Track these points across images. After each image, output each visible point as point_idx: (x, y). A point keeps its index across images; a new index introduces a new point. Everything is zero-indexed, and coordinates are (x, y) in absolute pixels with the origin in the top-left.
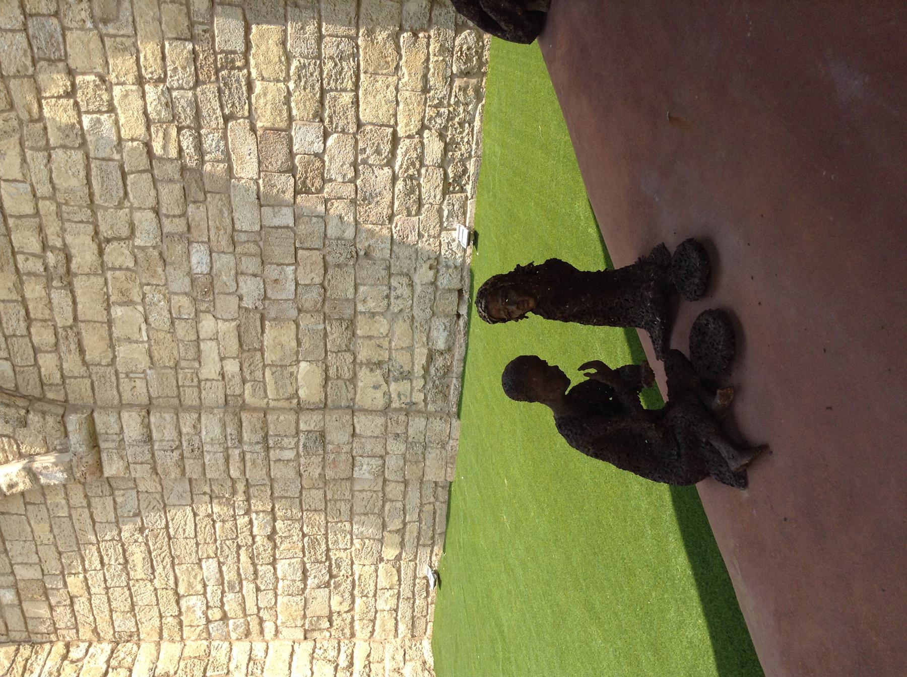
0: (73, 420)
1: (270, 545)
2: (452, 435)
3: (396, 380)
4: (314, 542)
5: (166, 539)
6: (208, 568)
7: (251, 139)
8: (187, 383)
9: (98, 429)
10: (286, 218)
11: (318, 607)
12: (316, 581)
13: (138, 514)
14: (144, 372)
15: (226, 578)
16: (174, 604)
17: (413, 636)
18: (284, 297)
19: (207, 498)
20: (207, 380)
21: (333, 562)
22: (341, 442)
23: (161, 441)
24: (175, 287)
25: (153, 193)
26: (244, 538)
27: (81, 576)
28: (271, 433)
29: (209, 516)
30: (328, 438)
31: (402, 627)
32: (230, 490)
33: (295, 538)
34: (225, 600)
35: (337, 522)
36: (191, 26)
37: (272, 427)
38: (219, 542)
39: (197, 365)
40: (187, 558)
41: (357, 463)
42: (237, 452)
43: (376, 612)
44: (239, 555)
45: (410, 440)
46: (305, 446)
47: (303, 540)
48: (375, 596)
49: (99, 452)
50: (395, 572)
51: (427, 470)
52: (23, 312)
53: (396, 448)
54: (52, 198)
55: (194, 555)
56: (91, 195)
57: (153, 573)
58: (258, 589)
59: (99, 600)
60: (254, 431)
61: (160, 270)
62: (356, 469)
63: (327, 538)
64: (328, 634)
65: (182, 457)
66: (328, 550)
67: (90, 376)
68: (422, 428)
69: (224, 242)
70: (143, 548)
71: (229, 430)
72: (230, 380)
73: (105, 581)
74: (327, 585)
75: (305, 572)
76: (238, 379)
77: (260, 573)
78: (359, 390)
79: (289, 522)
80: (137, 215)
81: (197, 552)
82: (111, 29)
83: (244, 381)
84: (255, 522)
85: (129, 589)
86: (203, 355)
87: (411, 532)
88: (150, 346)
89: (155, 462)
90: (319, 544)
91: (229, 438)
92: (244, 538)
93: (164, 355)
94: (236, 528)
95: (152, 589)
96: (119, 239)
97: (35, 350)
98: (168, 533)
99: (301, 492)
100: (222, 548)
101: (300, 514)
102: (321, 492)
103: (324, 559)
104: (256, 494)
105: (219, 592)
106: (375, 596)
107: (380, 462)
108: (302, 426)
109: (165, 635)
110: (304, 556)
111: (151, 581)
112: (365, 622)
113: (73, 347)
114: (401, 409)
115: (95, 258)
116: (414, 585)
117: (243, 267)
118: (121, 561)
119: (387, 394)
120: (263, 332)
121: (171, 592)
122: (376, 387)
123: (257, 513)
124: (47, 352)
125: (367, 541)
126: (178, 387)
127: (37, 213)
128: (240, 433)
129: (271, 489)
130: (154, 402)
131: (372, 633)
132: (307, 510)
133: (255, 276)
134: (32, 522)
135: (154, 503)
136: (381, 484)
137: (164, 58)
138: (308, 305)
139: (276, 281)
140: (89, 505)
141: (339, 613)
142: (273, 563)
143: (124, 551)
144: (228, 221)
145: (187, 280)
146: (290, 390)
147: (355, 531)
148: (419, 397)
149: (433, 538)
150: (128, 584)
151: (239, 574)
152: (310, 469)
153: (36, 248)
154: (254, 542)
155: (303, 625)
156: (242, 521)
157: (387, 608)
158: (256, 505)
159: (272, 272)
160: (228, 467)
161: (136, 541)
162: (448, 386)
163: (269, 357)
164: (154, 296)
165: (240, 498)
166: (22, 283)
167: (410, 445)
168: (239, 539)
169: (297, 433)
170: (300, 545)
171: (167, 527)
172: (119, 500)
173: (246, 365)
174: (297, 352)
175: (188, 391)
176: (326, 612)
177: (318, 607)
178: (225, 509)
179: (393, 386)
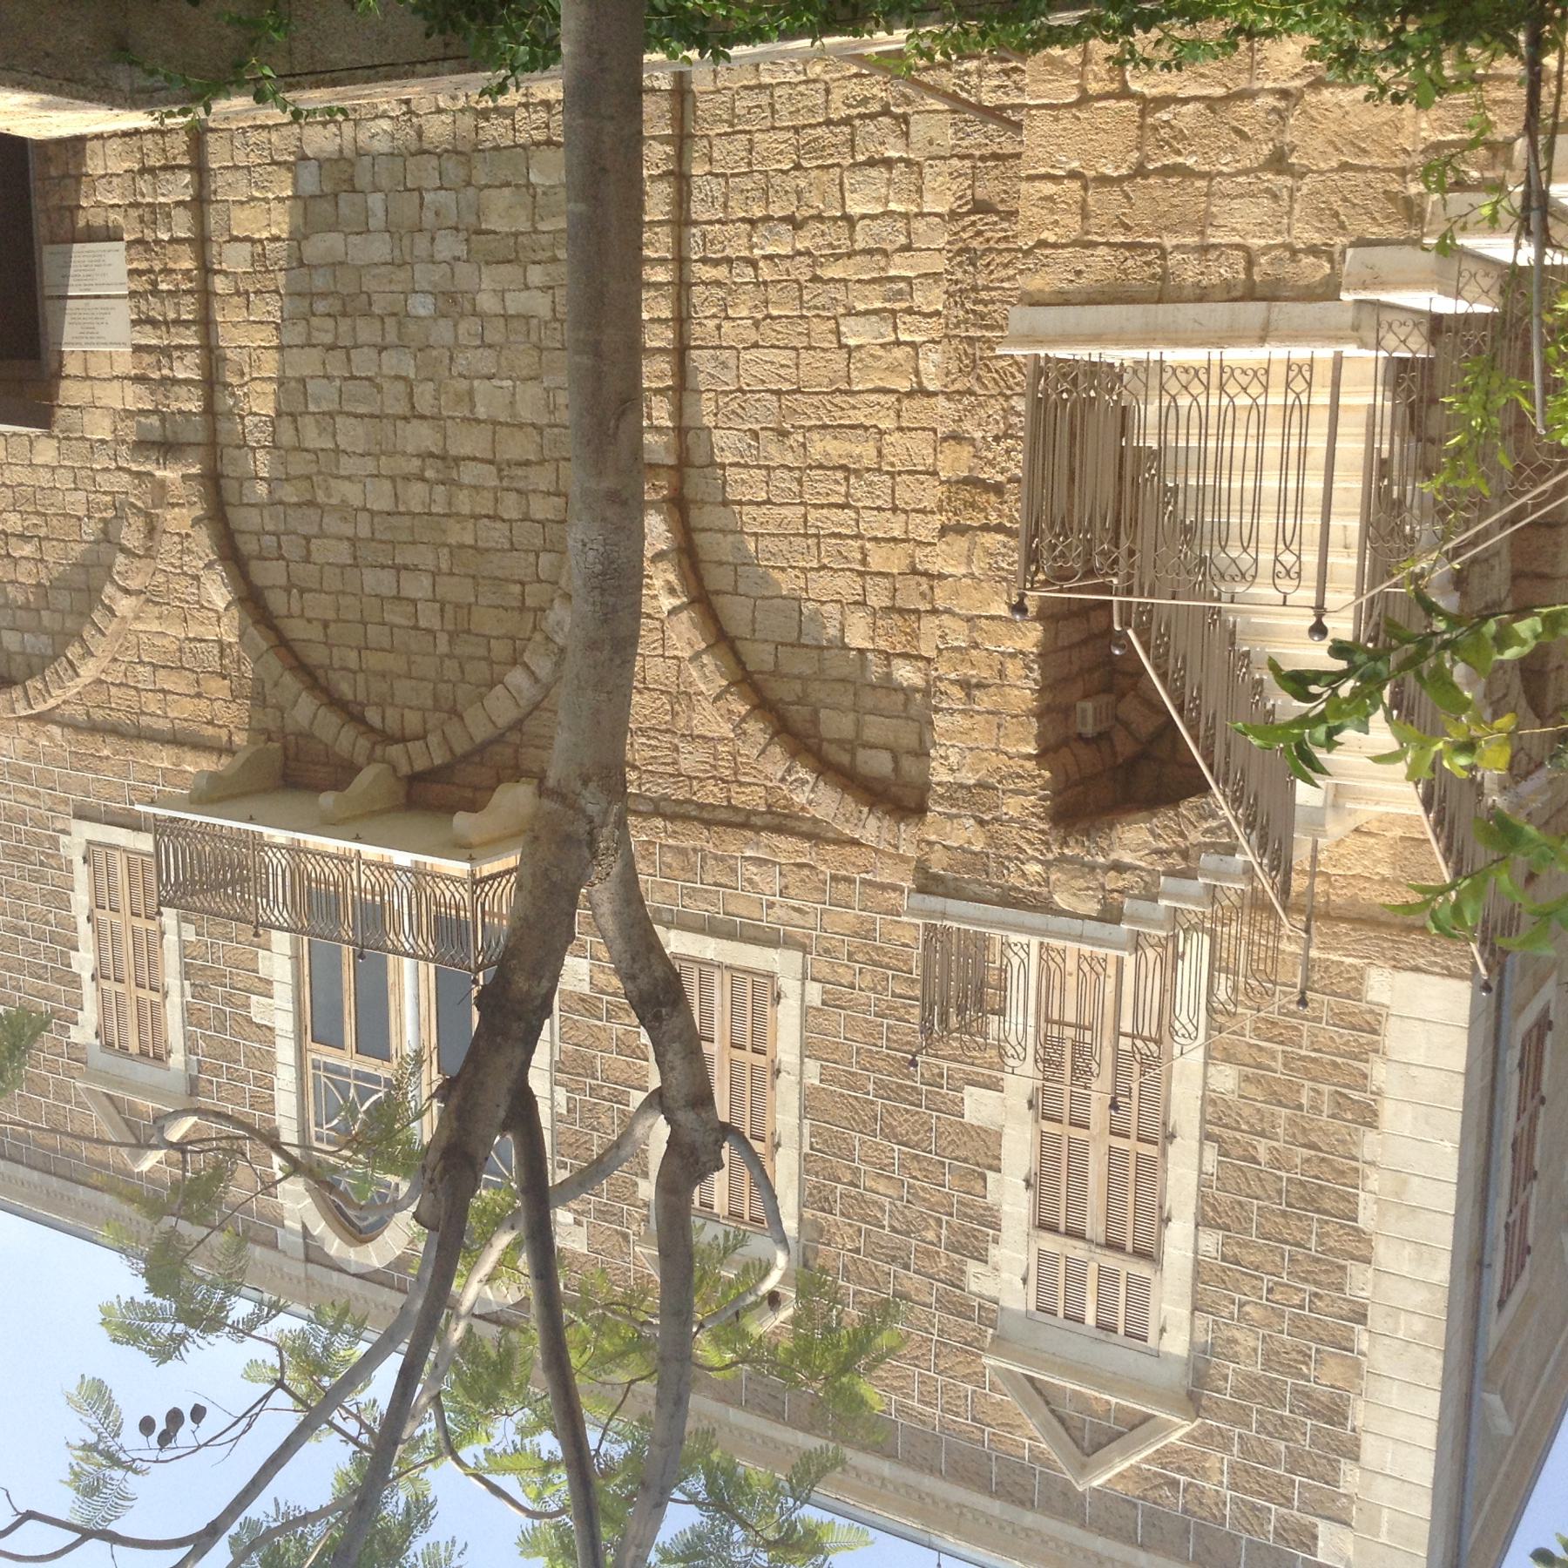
1: (815, 226)
5: (798, 396)
6: (856, 334)
7: (315, 238)
10: (376, 201)
12: (891, 140)
14: (547, 390)
15: (878, 305)
16: (933, 400)
18: (454, 205)
20: (554, 310)
21: (854, 112)
24: (448, 337)
25: (366, 349)
27: (868, 545)
29: (756, 324)
34: (926, 309)
35: (774, 111)
36: (238, 293)
38: (805, 312)
39: (535, 321)
40: (836, 367)
44: (832, 280)
47: (806, 169)
52: (486, 520)
54: (377, 457)
55: (828, 355)
56: (372, 416)
57: (866, 428)
58: (907, 248)
61: (435, 353)
63: (804, 127)
66: (829, 122)
67: (557, 460)
69: (402, 275)
70: (815, 436)
72: (553, 279)
73: (879, 509)
74: (905, 118)
75: (871, 163)
76: (551, 268)
79: (771, 192)
80: (385, 370)
81: (824, 350)
82: (246, 370)
84: (770, 250)
85: (900, 473)
86: (522, 311)
88: (518, 378)
90: (815, 140)
93: (526, 362)
94: (779, 282)
95: (897, 435)
96: (411, 395)
97: (526, 518)
98: (788, 392)
99: (717, 175)
100: (816, 308)
101: (757, 176)
103: (847, 130)
105: (908, 318)
110: (838, 165)
111: (881, 433)
113: (520, 472)
115: (425, 424)
117: (424, 254)
118: (840, 475)
120: (495, 232)
121: (906, 403)
123: (751, 248)
124: (528, 505)
127: (392, 478)
132: (750, 164)
133: (433, 239)
137: (262, 323)
138: (462, 173)
139: (437, 214)
143: (821, 467)
144: (383, 269)
145: (442, 322)
150: (888, 473)
151: (873, 281)
153: (418, 488)
154: (808, 253)
156: (766, 273)
159: (429, 218)
161: (804, 445)
163: (524, 226)
164: (461, 364)
166: (458, 514)
168: (802, 279)
170: (814, 173)
171: (778, 393)
174: (517, 186)
178: (743, 297)
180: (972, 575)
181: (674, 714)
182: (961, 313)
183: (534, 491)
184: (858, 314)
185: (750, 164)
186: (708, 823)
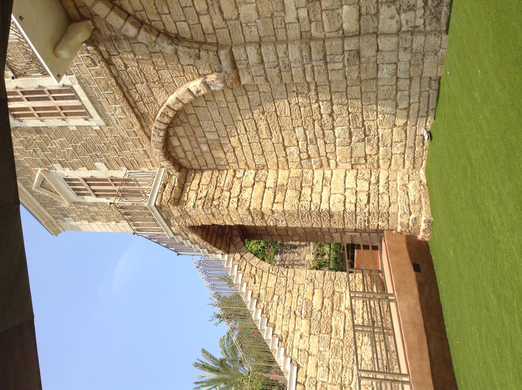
0: (223, 53)
2: (443, 46)
3: (405, 12)
4: (355, 117)
5: (276, 117)
6: (299, 132)
8: (279, 26)
9: (235, 57)
11: (358, 152)
12: (357, 138)
13: (260, 104)
14: (255, 22)
15: (308, 137)
16: (283, 151)
17: (414, 168)
19: (295, 94)
20: (290, 23)
21: (366, 128)
22: (370, 56)
23: (268, 62)
26: (316, 116)
27: (237, 137)
28: (328, 53)
29: (297, 104)
30: (362, 54)
31: (407, 163)
32: (307, 89)
33: (344, 115)
34: (309, 148)
35: (368, 105)
37: (328, 49)
38: (303, 118)
39: (283, 15)
40: (288, 127)
41: (380, 69)
42: (309, 66)
43: (392, 155)
44: (314, 125)
45: (414, 51)
46: (348, 60)
47: (349, 116)
48: (391, 146)
49: (238, 71)
50: (403, 132)
51: (425, 70)
53: (405, 57)
57: (271, 135)
58: (325, 143)
59: (247, 149)
60: (318, 53)
62: (379, 72)
63: (362, 114)
64: (364, 167)
65: (280, 71)
66: (363, 121)
67: (227, 27)
68: (422, 43)
70: (265, 122)
71: (304, 53)
72: (303, 22)
73: (248, 139)
74: (364, 140)
75: (350, 133)
76: (307, 21)
77: (326, 135)
78: (380, 21)
81: (292, 124)
83: (310, 22)
84: (322, 107)
85: (260, 143)
86: (286, 7)
87: (414, 109)
88: (257, 5)
89: (266, 74)
90: (358, 118)
91: (304, 58)
92: (316, 116)
94: (312, 110)
95: (272, 143)
97: (198, 14)
98: (277, 114)
99: (347, 88)
102: (359, 87)
103: (361, 126)
104: (321, 91)
105: (305, 144)
106: (391, 146)
107: (395, 67)
108: (346, 48)
109: (280, 166)
110: (350, 125)
111: (271, 139)
112: (385, 160)
113: (217, 10)
114: (408, 31)
116: (415, 140)
118: (255, 129)
119: (399, 22)
121: (281, 145)
122: (391, 18)
123: (322, 101)
124: (204, 15)
125: (386, 115)
126: (274, 29)
128: (310, 55)
129: (330, 87)
130: (262, 39)
131: (390, 166)
132: (351, 99)
134: (210, 110)
135: (268, 98)
136: (395, 80)
140: (236, 101)
141: (370, 155)
142: (333, 129)
143: (256, 124)
146: (338, 25)
147: (379, 109)
148: (420, 22)
149: (427, 112)
150: (260, 141)
151: (315, 135)
152: (351, 74)
154: (322, 118)
155: (351, 162)
157: (399, 152)
158: (322, 97)
160: (305, 76)
161: (261, 119)
162: (440, 13)
165: (313, 93)
167: (414, 54)
169: (343, 52)
170: (347, 119)
171: (276, 111)
172: (250, 97)
173: (311, 11)
175: (280, 31)
176: (363, 155)
177: (358, 152)
179: (403, 16)
180: (240, 215)
181: (154, 82)
182: (304, 213)
183: (211, 17)
184: (305, 132)
185: (351, 99)
186: (124, 96)
